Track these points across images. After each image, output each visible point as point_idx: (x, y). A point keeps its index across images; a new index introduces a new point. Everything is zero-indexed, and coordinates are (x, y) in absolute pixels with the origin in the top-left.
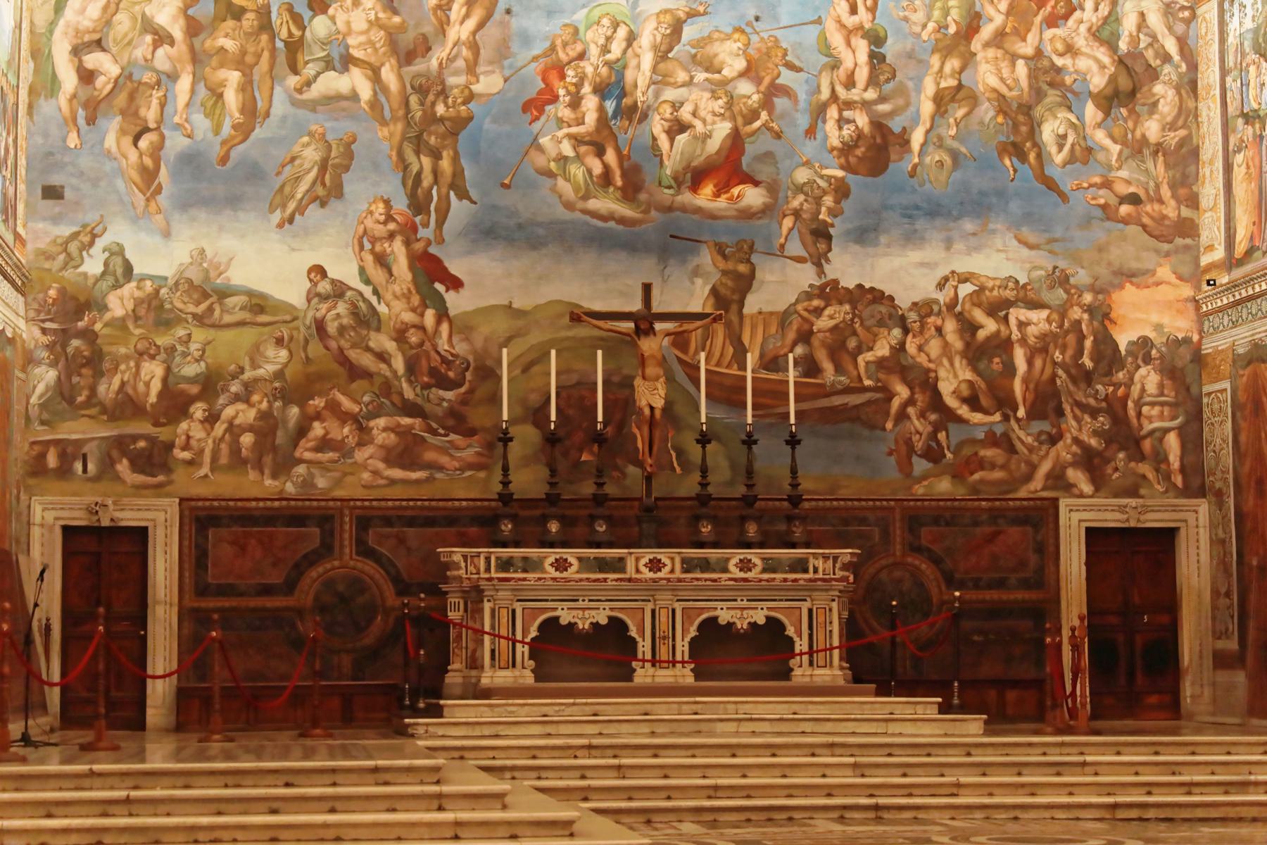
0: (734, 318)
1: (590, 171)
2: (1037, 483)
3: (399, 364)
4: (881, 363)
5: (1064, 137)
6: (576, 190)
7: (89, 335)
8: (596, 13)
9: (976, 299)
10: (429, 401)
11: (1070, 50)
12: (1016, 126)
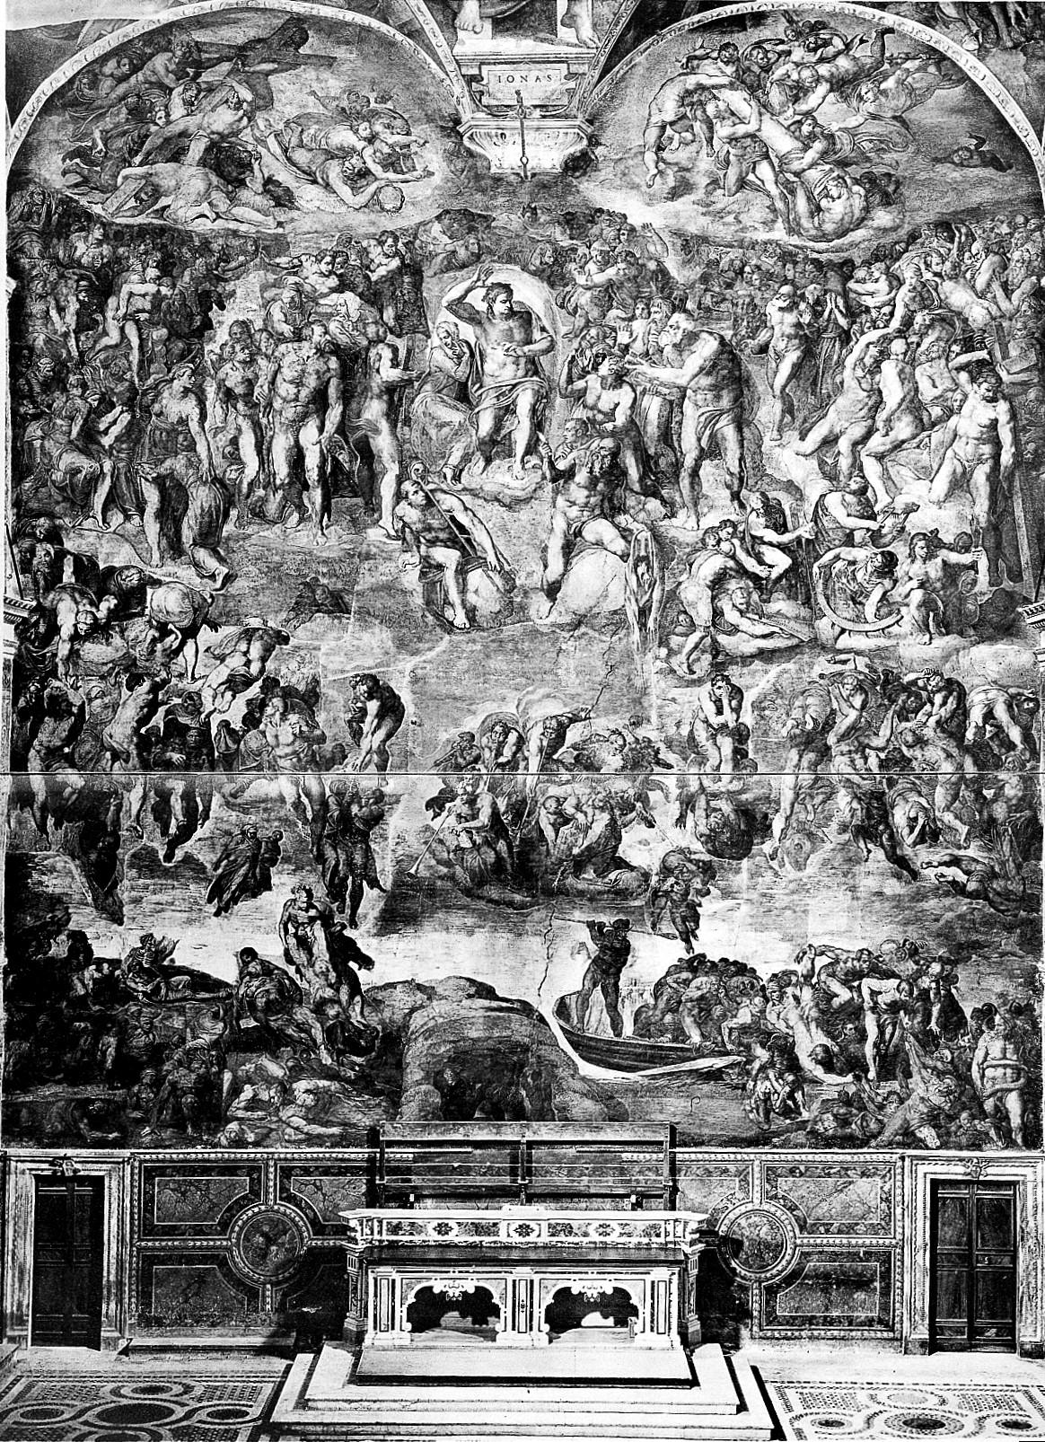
3: (318, 1034)
4: (744, 1029)
5: (915, 819)
11: (920, 742)
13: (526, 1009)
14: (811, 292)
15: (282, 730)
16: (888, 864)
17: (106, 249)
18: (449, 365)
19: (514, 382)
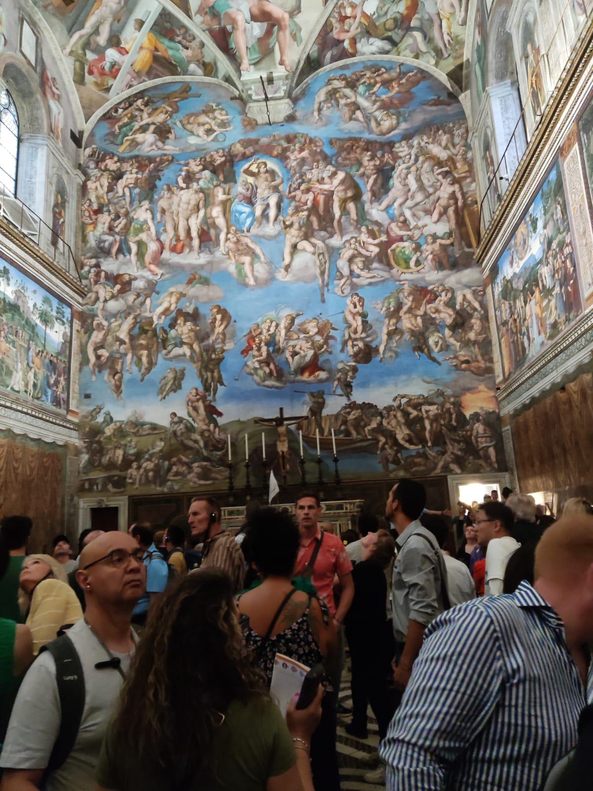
0: (318, 418)
1: (265, 372)
2: (438, 471)
3: (202, 444)
4: (373, 430)
5: (438, 342)
6: (261, 378)
7: (99, 442)
8: (265, 318)
9: (408, 403)
10: (212, 455)
11: (437, 311)
12: (419, 340)
15: (184, 329)
17: (118, 164)
18: (244, 191)
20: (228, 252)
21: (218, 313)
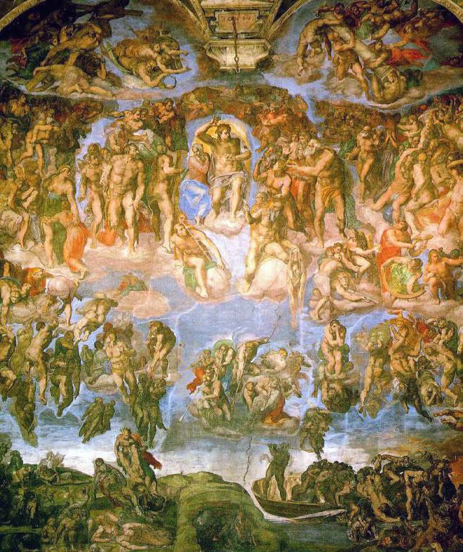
3: (135, 500)
4: (346, 496)
5: (431, 392)
9: (389, 466)
11: (435, 353)
13: (239, 488)
14: (379, 128)
15: (114, 350)
16: (417, 415)
17: (27, 108)
18: (198, 165)
19: (230, 174)
20: (175, 249)
21: (158, 331)
